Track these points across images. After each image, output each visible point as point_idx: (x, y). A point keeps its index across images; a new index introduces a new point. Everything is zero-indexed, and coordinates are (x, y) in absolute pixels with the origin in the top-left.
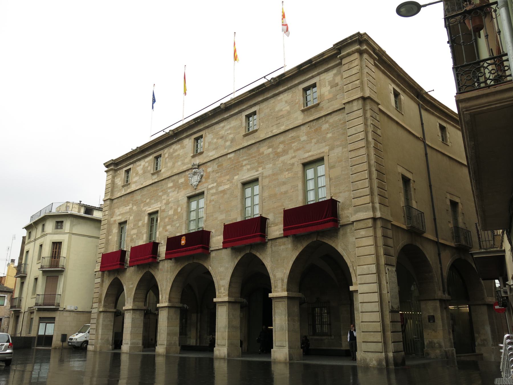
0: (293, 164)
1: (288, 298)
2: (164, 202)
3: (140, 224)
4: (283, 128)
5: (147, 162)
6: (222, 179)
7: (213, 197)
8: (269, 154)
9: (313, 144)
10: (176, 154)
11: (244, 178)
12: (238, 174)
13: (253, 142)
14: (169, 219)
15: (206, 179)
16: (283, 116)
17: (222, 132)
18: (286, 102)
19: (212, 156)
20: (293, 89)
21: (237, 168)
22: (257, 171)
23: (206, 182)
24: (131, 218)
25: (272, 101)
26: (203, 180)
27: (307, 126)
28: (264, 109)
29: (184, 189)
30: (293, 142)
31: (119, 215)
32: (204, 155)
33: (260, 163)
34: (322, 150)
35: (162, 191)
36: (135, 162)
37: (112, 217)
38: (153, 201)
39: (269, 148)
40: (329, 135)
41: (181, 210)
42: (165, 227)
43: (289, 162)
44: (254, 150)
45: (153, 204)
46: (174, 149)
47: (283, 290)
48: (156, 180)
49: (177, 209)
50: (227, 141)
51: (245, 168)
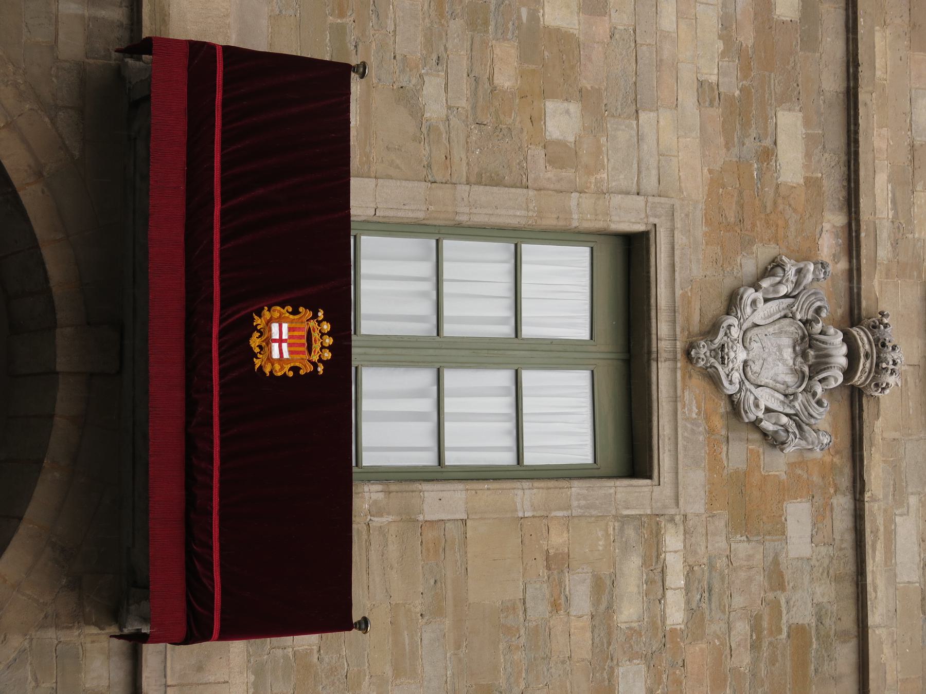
7: (581, 600)
23: (711, 501)
29: (715, 183)
41: (560, 155)
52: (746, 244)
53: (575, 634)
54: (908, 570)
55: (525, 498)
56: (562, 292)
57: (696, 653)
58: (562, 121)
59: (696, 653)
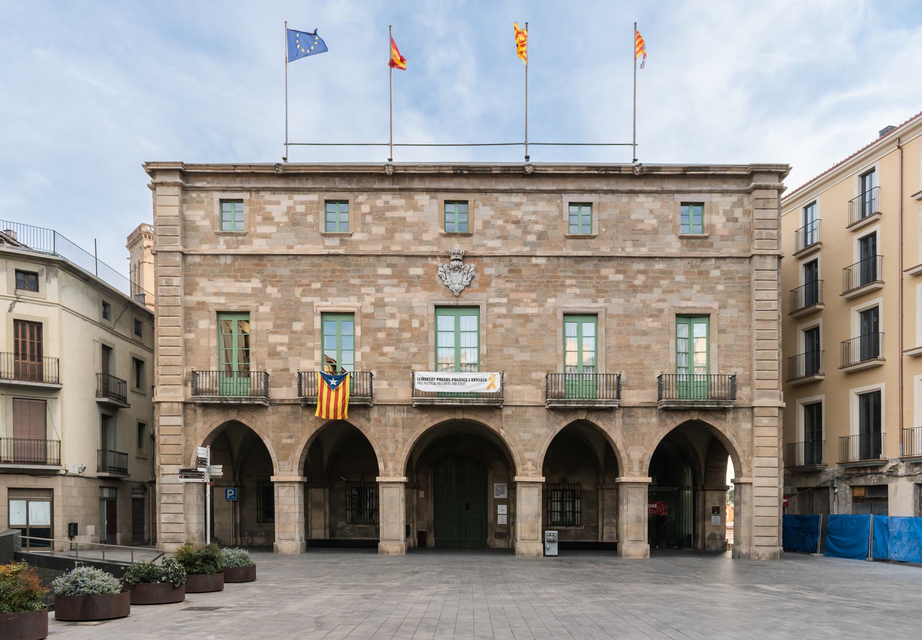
0: (661, 311)
1: (650, 485)
2: (369, 300)
3: (297, 326)
4: (644, 251)
5: (302, 203)
6: (521, 295)
8: (618, 282)
9: (694, 291)
10: (396, 214)
11: (567, 305)
12: (555, 296)
13: (589, 253)
14: (388, 335)
15: (481, 285)
16: (646, 233)
17: (517, 214)
18: (651, 211)
19: (495, 249)
20: (664, 196)
21: (552, 285)
22: (595, 302)
23: (484, 291)
24: (265, 309)
25: (625, 199)
26: (475, 285)
27: (686, 261)
28: (610, 206)
29: (424, 289)
30: (664, 278)
31: (216, 294)
32: (475, 240)
33: (601, 292)
34: (710, 305)
35: (359, 277)
36: (258, 190)
37: (191, 294)
38: (330, 290)
39: (618, 272)
40: (721, 287)
41: (422, 324)
42: (377, 347)
43: (654, 305)
44: (588, 266)
45: (331, 295)
46: (386, 203)
47: (643, 474)
48: (341, 251)
49: (409, 322)
50: (529, 233)
51: (568, 290)
52: (435, 282)
53: (508, 323)
54: (497, 243)
55: (483, 333)
56: (446, 321)
57: (513, 296)
58: (415, 324)
59: (513, 296)
